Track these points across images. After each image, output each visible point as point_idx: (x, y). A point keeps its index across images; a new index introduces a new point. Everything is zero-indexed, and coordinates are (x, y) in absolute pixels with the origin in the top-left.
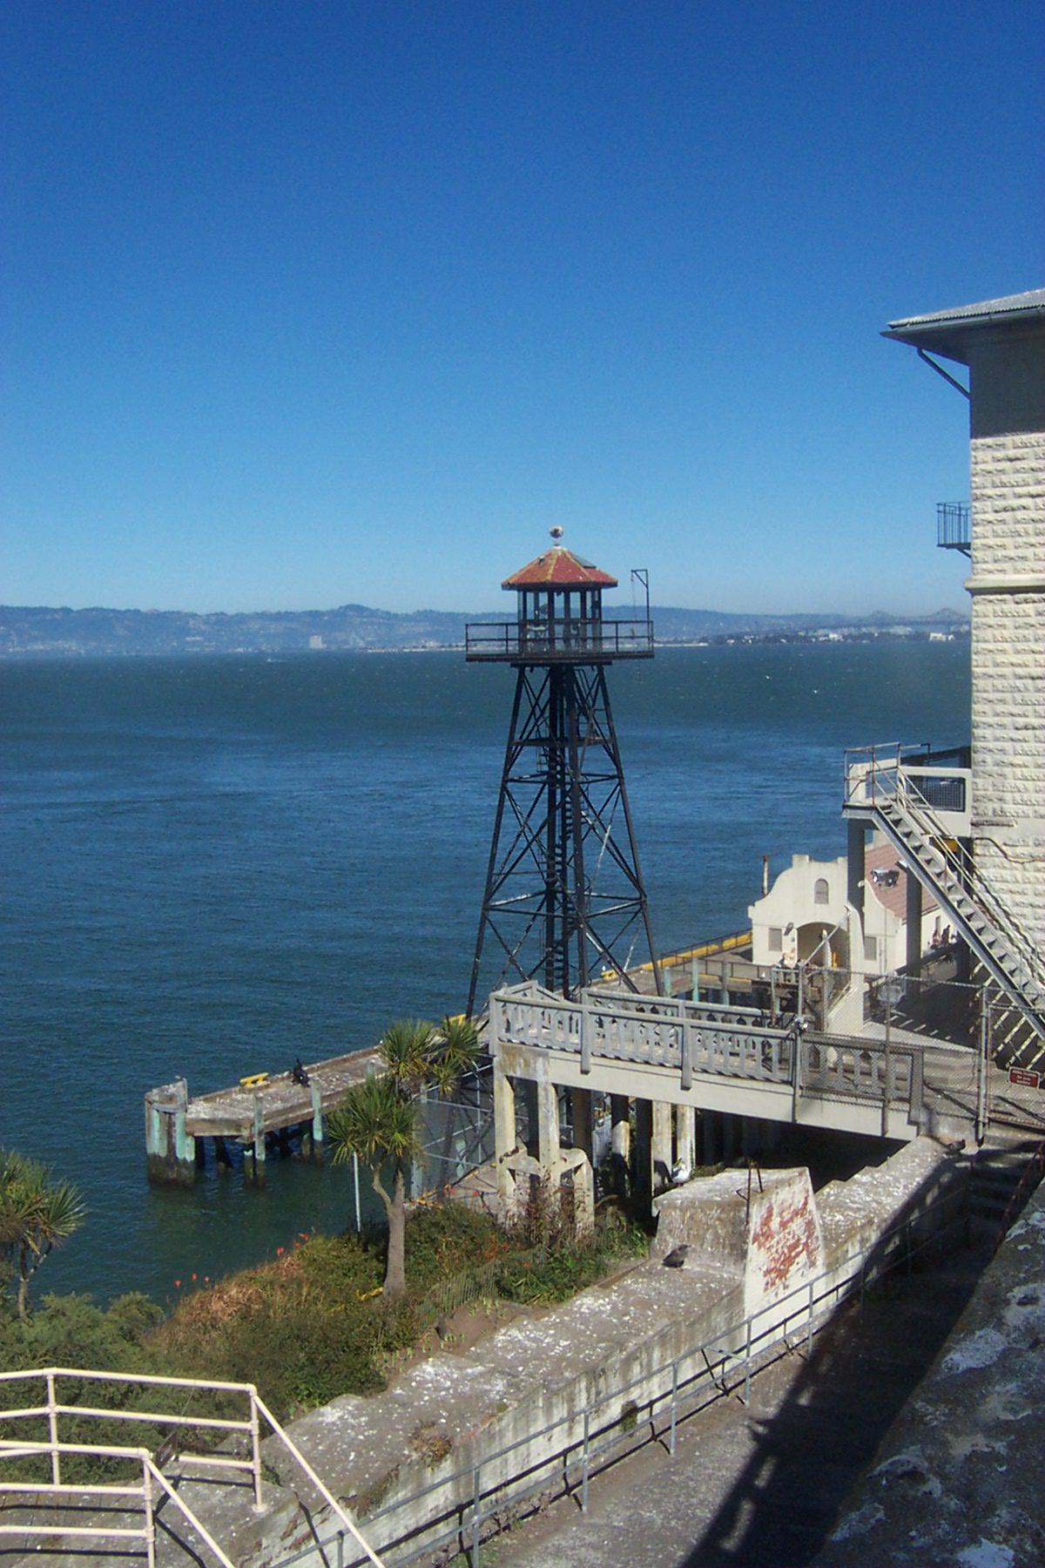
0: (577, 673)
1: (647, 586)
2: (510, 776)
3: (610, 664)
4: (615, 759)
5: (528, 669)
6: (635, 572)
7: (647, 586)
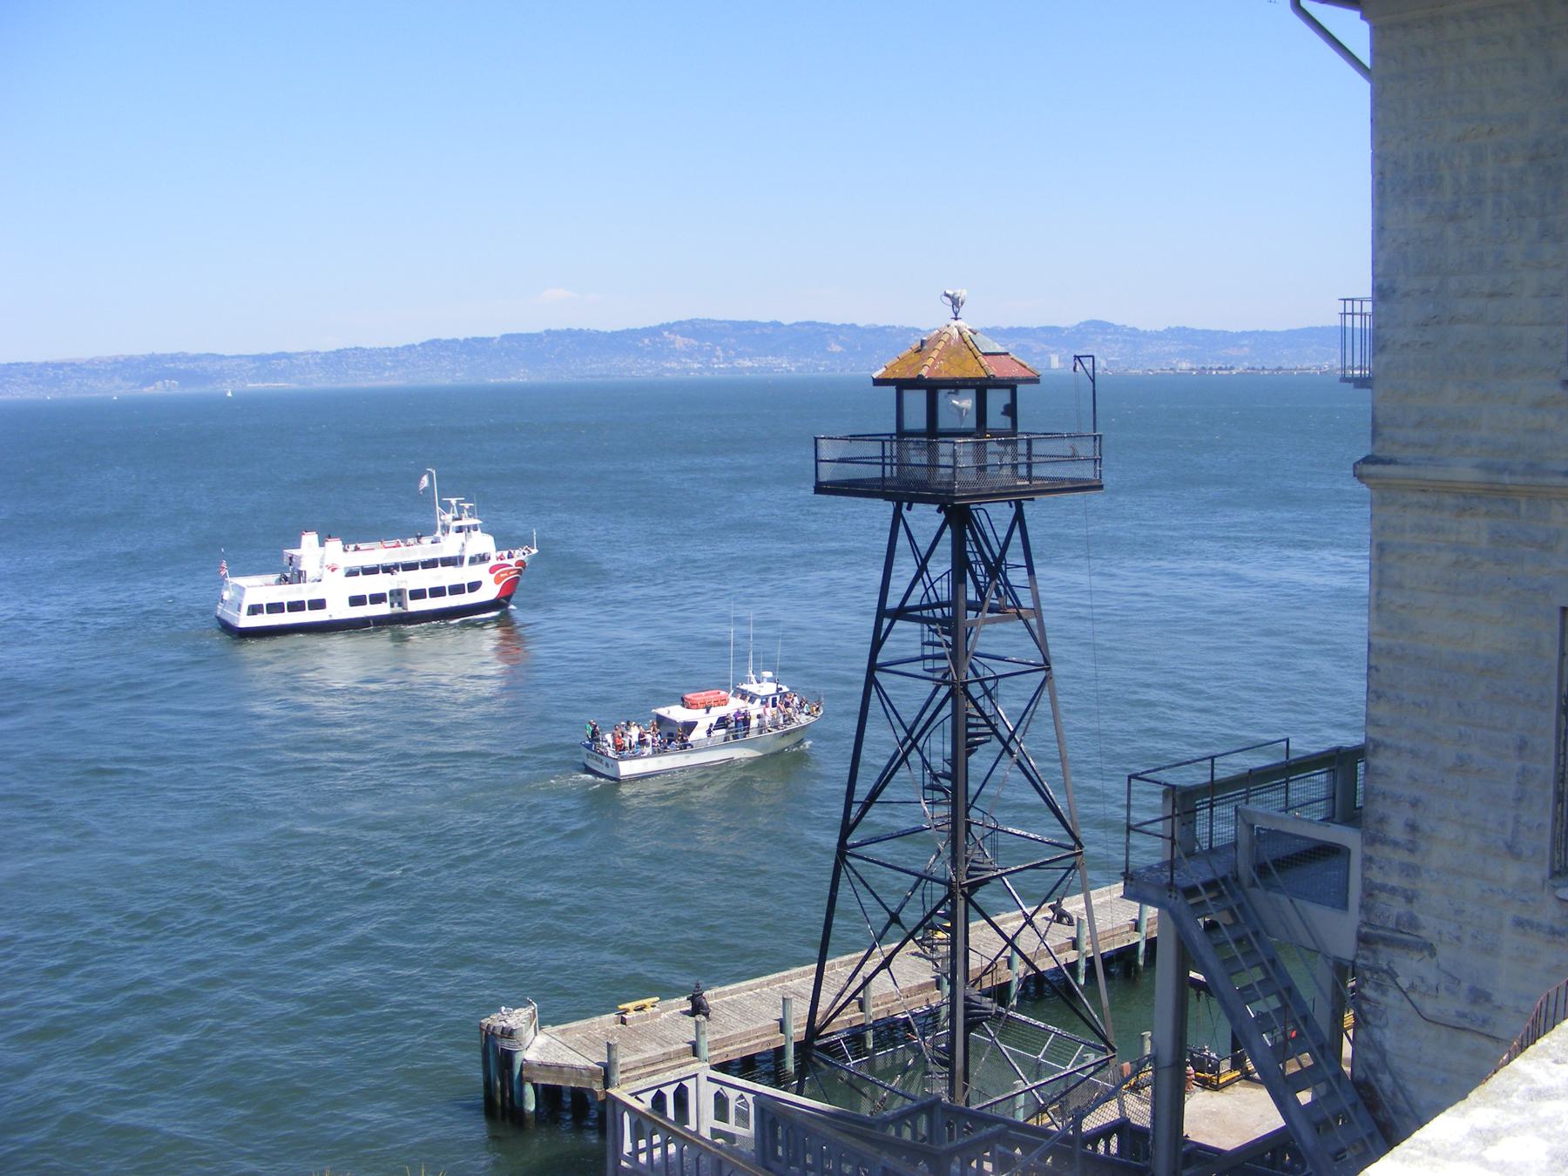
0: (974, 512)
1: (1093, 381)
2: (879, 661)
3: (1033, 499)
4: (1042, 646)
5: (905, 504)
6: (1079, 357)
7: (1093, 381)
